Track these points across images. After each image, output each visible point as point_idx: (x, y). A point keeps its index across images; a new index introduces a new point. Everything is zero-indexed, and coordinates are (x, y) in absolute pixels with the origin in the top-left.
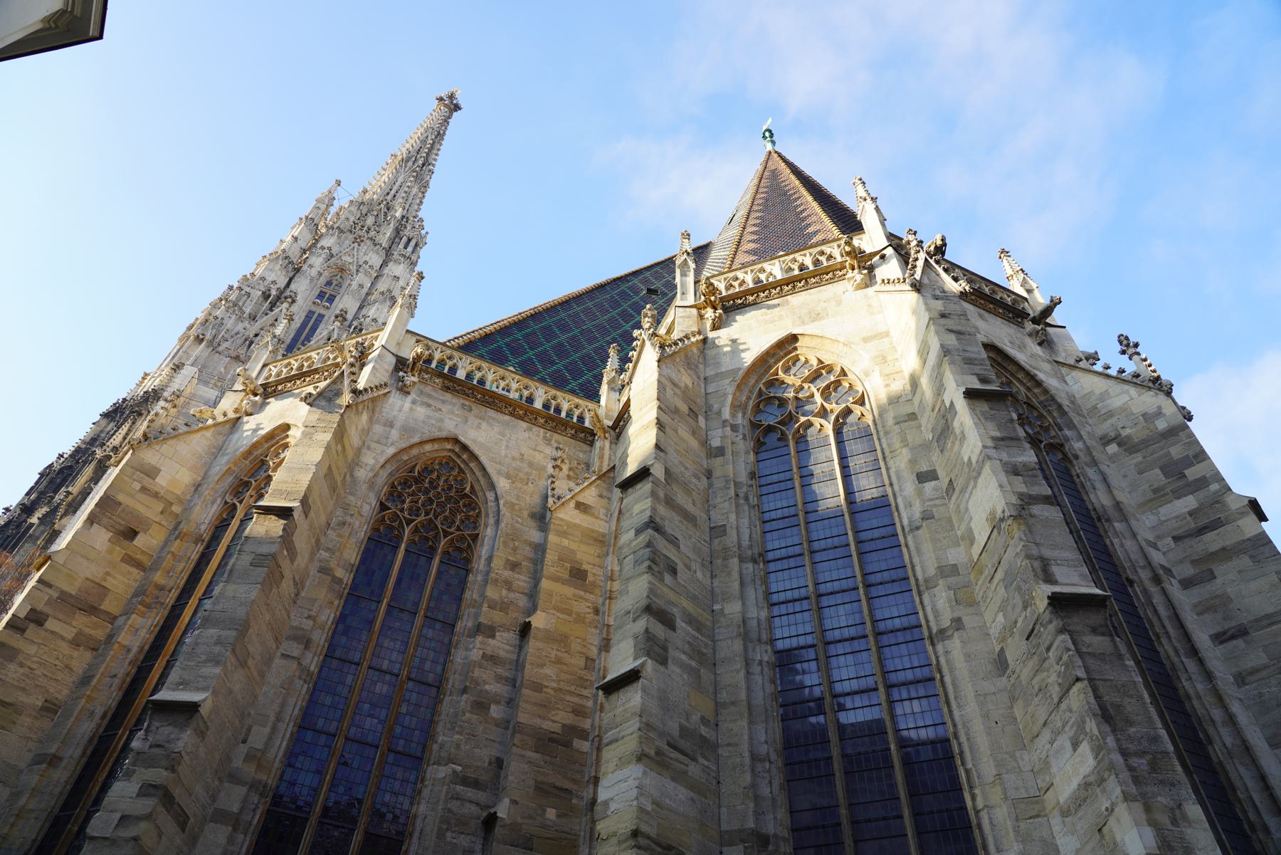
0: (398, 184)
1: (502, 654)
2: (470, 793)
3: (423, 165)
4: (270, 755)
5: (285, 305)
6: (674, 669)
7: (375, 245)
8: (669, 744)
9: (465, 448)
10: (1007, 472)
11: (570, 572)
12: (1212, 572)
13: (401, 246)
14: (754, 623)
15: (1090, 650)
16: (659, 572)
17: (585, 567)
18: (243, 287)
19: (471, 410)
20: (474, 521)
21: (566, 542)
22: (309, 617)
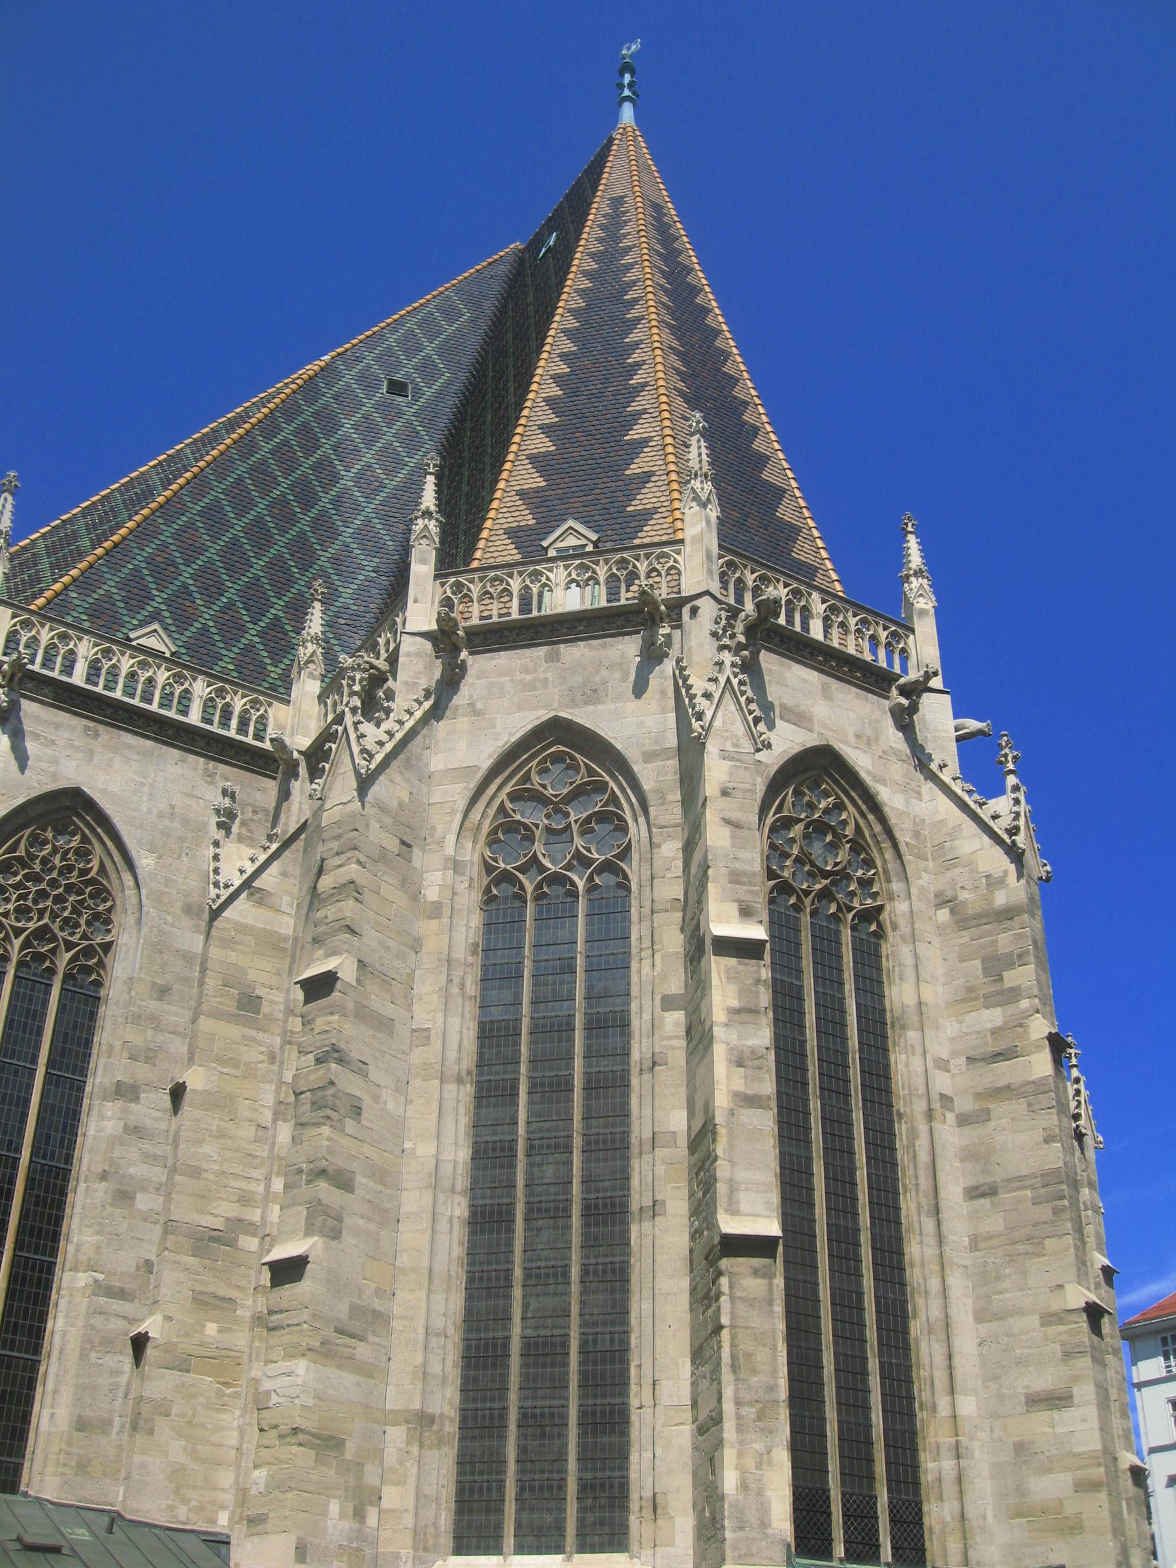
1: (149, 1123)
2: (117, 1305)
6: (348, 1239)
8: (337, 1331)
10: (730, 1061)
11: (239, 1001)
12: (988, 1111)
15: (744, 1294)
16: (339, 1121)
17: (258, 992)
19: (97, 735)
20: (104, 920)
21: (233, 956)
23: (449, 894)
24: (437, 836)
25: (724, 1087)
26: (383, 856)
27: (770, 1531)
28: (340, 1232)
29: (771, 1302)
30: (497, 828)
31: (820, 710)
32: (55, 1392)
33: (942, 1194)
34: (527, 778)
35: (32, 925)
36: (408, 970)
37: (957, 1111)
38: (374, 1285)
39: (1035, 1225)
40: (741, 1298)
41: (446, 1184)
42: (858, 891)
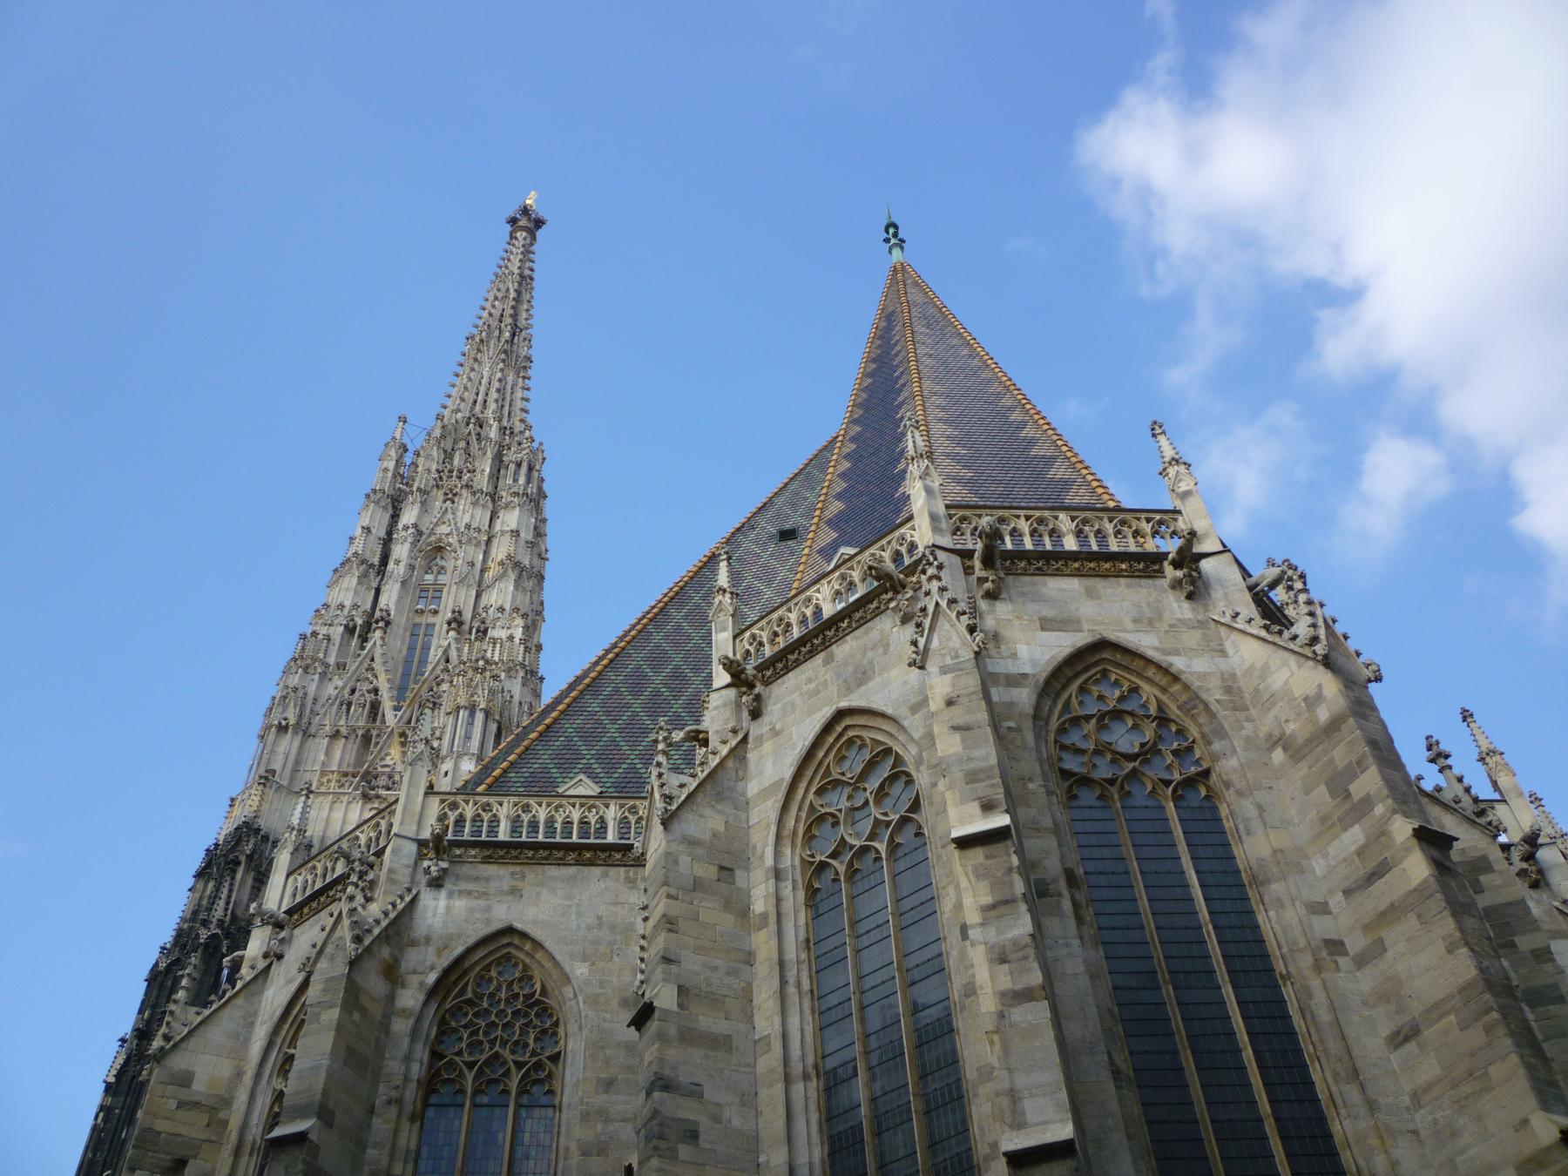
3: (513, 335)
5: (378, 634)
10: (991, 961)
12: (1381, 941)
16: (670, 1149)
19: (524, 877)
20: (550, 1033)
23: (772, 901)
24: (758, 852)
25: (989, 990)
26: (697, 885)
30: (810, 827)
31: (1087, 610)
33: (1356, 1052)
34: (828, 772)
35: (483, 1057)
36: (742, 984)
37: (1351, 954)
39: (1472, 1055)
42: (1176, 762)
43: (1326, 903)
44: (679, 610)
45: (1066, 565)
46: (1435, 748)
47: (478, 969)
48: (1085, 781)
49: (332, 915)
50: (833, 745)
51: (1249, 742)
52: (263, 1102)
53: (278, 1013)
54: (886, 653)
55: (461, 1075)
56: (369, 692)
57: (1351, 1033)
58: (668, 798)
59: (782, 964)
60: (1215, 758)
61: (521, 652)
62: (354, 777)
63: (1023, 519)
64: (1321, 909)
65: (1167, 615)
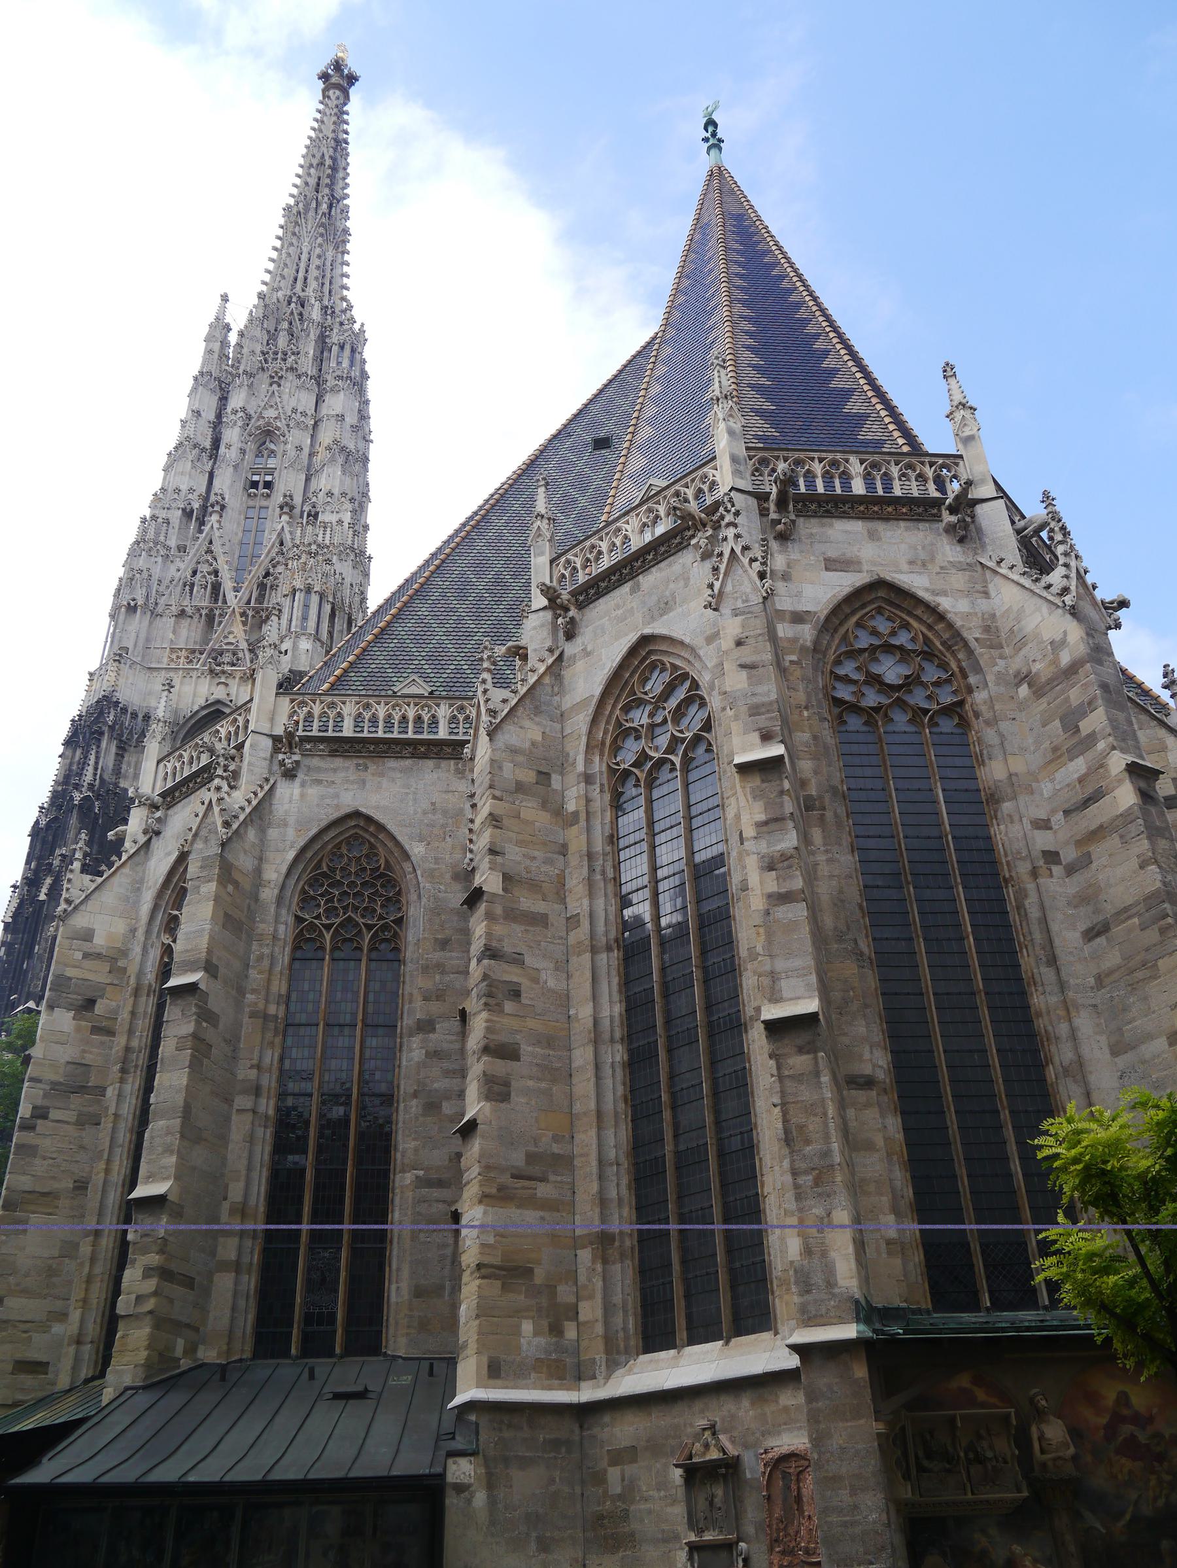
0: (304, 257)
1: (445, 1046)
2: (436, 1193)
3: (330, 206)
4: (252, 1201)
5: (215, 517)
6: (518, 1100)
7: (299, 377)
8: (514, 1176)
9: (369, 819)
10: (762, 868)
12: (1089, 854)
13: (333, 364)
14: (607, 1022)
15: (791, 1072)
16: (497, 1005)
18: (157, 512)
19: (366, 768)
20: (395, 900)
22: (252, 1067)
23: (583, 802)
24: (571, 760)
25: (759, 892)
26: (520, 787)
27: (836, 1290)
28: (509, 1094)
29: (817, 1074)
32: (398, 1270)
33: (1057, 942)
35: (338, 920)
36: (557, 871)
38: (550, 1134)
39: (1147, 950)
40: (789, 1076)
41: (606, 1036)
43: (1049, 820)
44: (499, 518)
45: (852, 508)
46: (1170, 676)
47: (330, 847)
48: (855, 708)
49: (203, 803)
50: (638, 667)
51: (1000, 676)
52: (155, 954)
53: (161, 881)
54: (686, 585)
55: (321, 935)
56: (209, 573)
57: (1055, 927)
58: (492, 713)
59: (590, 856)
60: (970, 690)
61: (350, 536)
62: (202, 653)
63: (817, 461)
64: (1043, 825)
65: (939, 557)
